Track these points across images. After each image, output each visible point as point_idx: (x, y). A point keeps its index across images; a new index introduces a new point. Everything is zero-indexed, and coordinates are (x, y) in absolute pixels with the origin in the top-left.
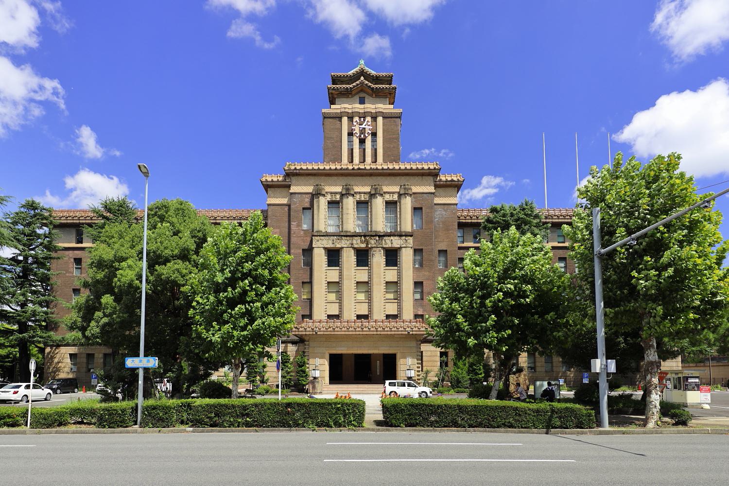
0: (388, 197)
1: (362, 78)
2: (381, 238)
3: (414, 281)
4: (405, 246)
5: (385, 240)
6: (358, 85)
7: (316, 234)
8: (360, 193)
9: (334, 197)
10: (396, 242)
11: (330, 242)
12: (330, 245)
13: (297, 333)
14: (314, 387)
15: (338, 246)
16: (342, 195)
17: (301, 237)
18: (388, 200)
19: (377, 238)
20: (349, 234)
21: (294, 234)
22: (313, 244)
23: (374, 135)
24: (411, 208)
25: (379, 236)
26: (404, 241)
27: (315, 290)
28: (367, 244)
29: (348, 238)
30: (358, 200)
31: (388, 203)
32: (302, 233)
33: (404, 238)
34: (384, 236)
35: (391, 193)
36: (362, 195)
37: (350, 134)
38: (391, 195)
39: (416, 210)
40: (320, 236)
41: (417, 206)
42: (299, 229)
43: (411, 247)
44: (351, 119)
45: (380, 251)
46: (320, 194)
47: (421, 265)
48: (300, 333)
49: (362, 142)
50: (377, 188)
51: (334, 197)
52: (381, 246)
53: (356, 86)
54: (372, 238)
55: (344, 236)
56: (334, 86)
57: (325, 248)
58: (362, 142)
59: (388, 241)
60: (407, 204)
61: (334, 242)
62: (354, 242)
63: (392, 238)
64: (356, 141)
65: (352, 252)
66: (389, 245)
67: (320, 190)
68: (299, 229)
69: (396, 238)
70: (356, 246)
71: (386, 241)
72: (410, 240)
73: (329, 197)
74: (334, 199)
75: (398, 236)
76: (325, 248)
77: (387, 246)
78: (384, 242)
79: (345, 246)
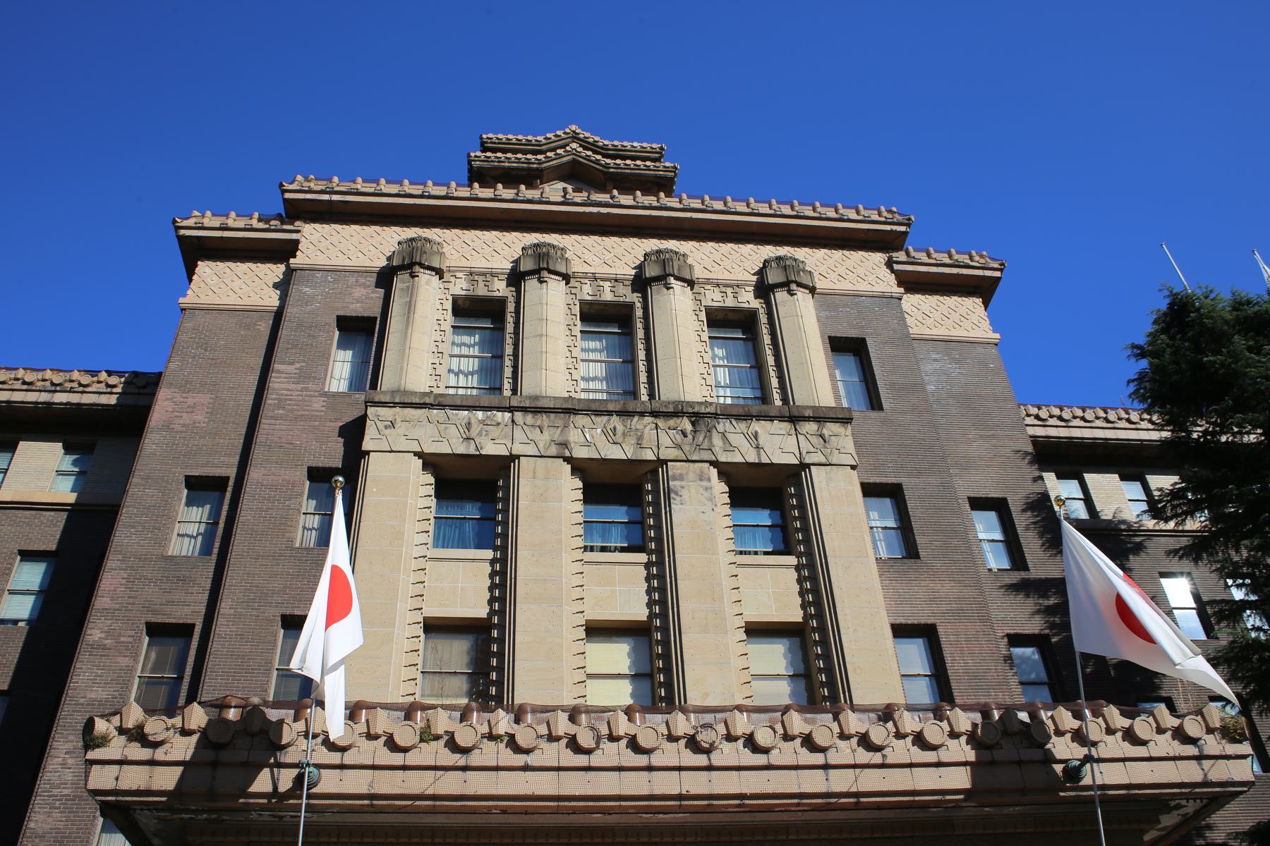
0: (714, 298)
2: (702, 427)
3: (893, 621)
4: (823, 460)
5: (723, 435)
7: (387, 399)
8: (595, 278)
9: (481, 284)
18: (715, 304)
19: (686, 425)
22: (367, 438)
25: (697, 417)
26: (815, 440)
28: (639, 444)
29: (544, 420)
31: (719, 320)
32: (318, 404)
33: (811, 427)
34: (715, 416)
35: (726, 286)
36: (607, 284)
38: (729, 290)
40: (405, 405)
42: (307, 389)
43: (853, 467)
45: (702, 477)
47: (911, 552)
52: (707, 456)
54: (661, 423)
55: (524, 410)
57: (430, 462)
61: (474, 433)
62: (574, 436)
63: (757, 426)
65: (570, 487)
68: (307, 389)
69: (782, 427)
70: (581, 453)
71: (730, 437)
72: (843, 440)
73: (460, 287)
74: (481, 291)
75: (781, 418)
76: (430, 462)
77: (738, 459)
78: (717, 441)
79: (531, 450)
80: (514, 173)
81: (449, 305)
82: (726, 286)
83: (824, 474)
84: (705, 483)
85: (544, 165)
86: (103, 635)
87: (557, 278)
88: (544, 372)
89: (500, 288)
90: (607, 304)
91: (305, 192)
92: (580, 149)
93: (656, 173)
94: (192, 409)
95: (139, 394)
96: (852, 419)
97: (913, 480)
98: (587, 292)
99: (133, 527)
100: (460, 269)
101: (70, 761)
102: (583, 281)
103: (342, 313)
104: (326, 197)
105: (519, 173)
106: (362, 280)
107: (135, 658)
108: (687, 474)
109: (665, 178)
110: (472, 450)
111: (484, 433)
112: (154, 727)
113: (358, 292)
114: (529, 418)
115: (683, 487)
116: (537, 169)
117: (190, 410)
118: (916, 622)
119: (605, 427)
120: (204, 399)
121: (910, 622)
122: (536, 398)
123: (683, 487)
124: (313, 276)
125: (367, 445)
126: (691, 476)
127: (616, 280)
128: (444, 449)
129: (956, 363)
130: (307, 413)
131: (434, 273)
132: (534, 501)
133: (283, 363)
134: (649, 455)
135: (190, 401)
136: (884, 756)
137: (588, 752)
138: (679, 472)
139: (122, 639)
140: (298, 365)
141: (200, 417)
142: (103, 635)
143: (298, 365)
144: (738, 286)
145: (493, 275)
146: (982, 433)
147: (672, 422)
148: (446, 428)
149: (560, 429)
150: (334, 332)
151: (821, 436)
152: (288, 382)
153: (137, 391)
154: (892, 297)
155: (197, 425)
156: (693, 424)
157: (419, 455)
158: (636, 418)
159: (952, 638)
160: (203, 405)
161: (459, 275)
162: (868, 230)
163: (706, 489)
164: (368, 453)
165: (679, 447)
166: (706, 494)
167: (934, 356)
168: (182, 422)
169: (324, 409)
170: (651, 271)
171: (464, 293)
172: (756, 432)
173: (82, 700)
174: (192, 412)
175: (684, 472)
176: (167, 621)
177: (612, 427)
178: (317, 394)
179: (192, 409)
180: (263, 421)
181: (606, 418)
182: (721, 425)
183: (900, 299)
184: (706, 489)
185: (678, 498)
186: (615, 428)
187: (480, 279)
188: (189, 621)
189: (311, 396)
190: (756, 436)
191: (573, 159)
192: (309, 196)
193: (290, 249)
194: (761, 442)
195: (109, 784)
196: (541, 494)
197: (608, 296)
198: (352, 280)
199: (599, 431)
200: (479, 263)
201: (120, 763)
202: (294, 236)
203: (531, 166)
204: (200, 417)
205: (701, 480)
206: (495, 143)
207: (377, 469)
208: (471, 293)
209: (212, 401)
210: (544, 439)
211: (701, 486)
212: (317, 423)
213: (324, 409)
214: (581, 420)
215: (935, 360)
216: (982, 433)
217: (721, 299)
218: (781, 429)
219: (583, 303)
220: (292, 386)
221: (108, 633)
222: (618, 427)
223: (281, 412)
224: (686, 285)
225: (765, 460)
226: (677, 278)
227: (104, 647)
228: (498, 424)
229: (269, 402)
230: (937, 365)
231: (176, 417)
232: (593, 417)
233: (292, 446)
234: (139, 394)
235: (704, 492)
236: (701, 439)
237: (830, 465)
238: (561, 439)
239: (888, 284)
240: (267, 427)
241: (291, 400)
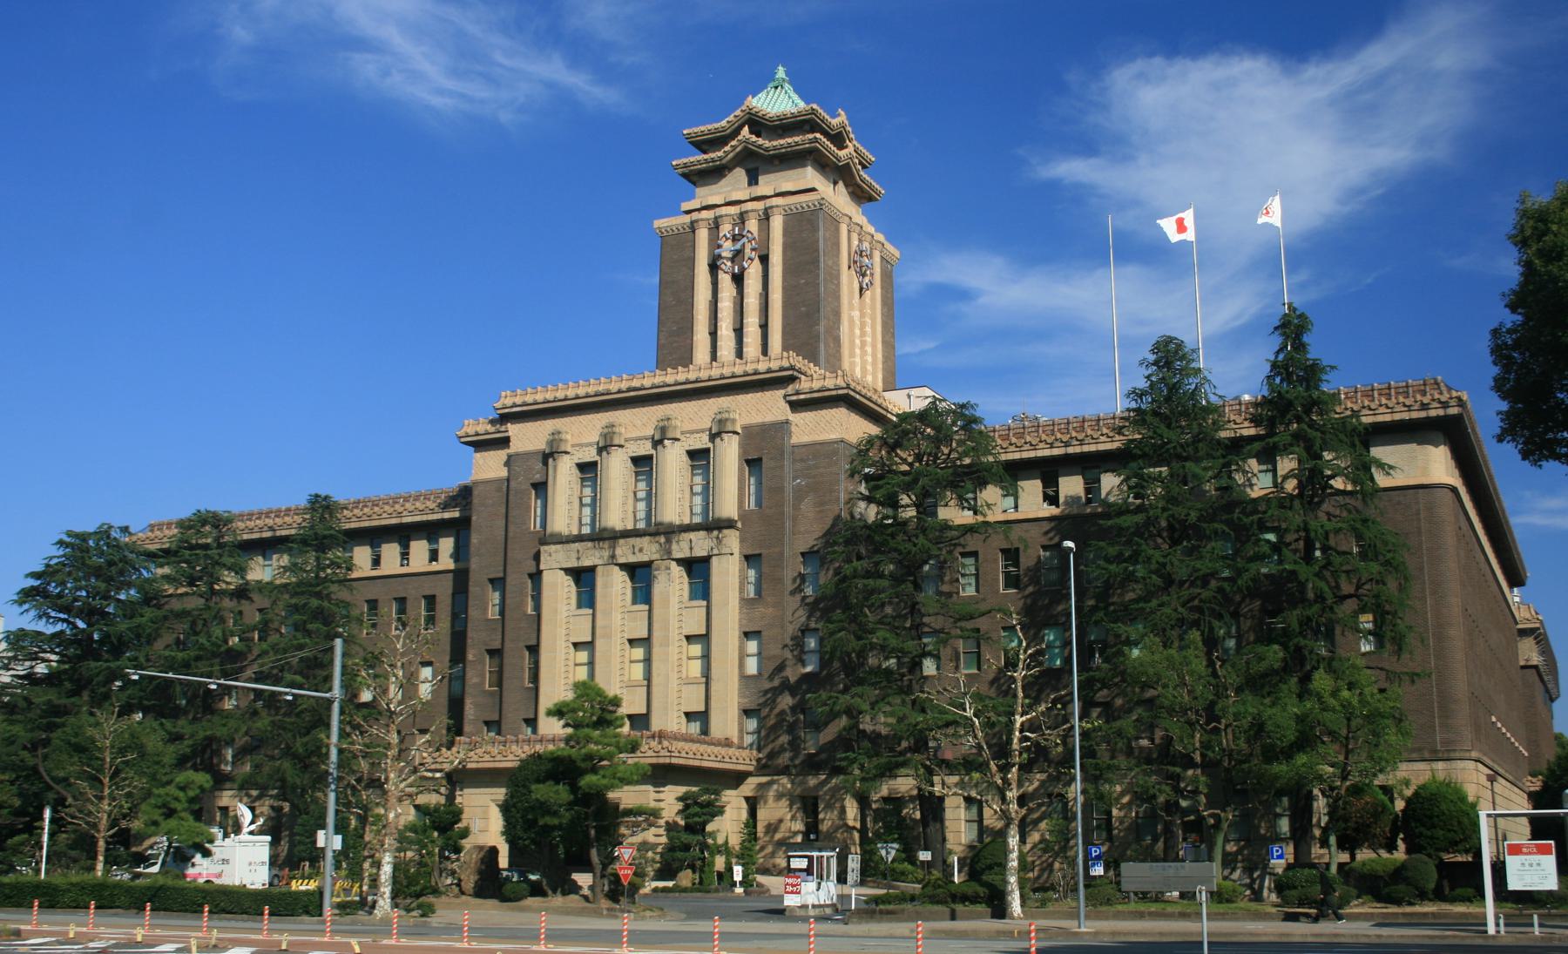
6: (734, 147)
10: (700, 544)
11: (574, 555)
12: (573, 564)
15: (587, 563)
19: (662, 539)
23: (764, 259)
37: (714, 268)
39: (752, 463)
49: (738, 279)
57: (568, 571)
58: (738, 279)
60: (673, 461)
64: (725, 280)
69: (702, 533)
76: (568, 571)
107: (484, 665)
126: (663, 568)
147: (657, 538)
150: (530, 493)
157: (561, 569)
193: (504, 442)
202: (506, 434)
210: (606, 554)
221: (474, 655)
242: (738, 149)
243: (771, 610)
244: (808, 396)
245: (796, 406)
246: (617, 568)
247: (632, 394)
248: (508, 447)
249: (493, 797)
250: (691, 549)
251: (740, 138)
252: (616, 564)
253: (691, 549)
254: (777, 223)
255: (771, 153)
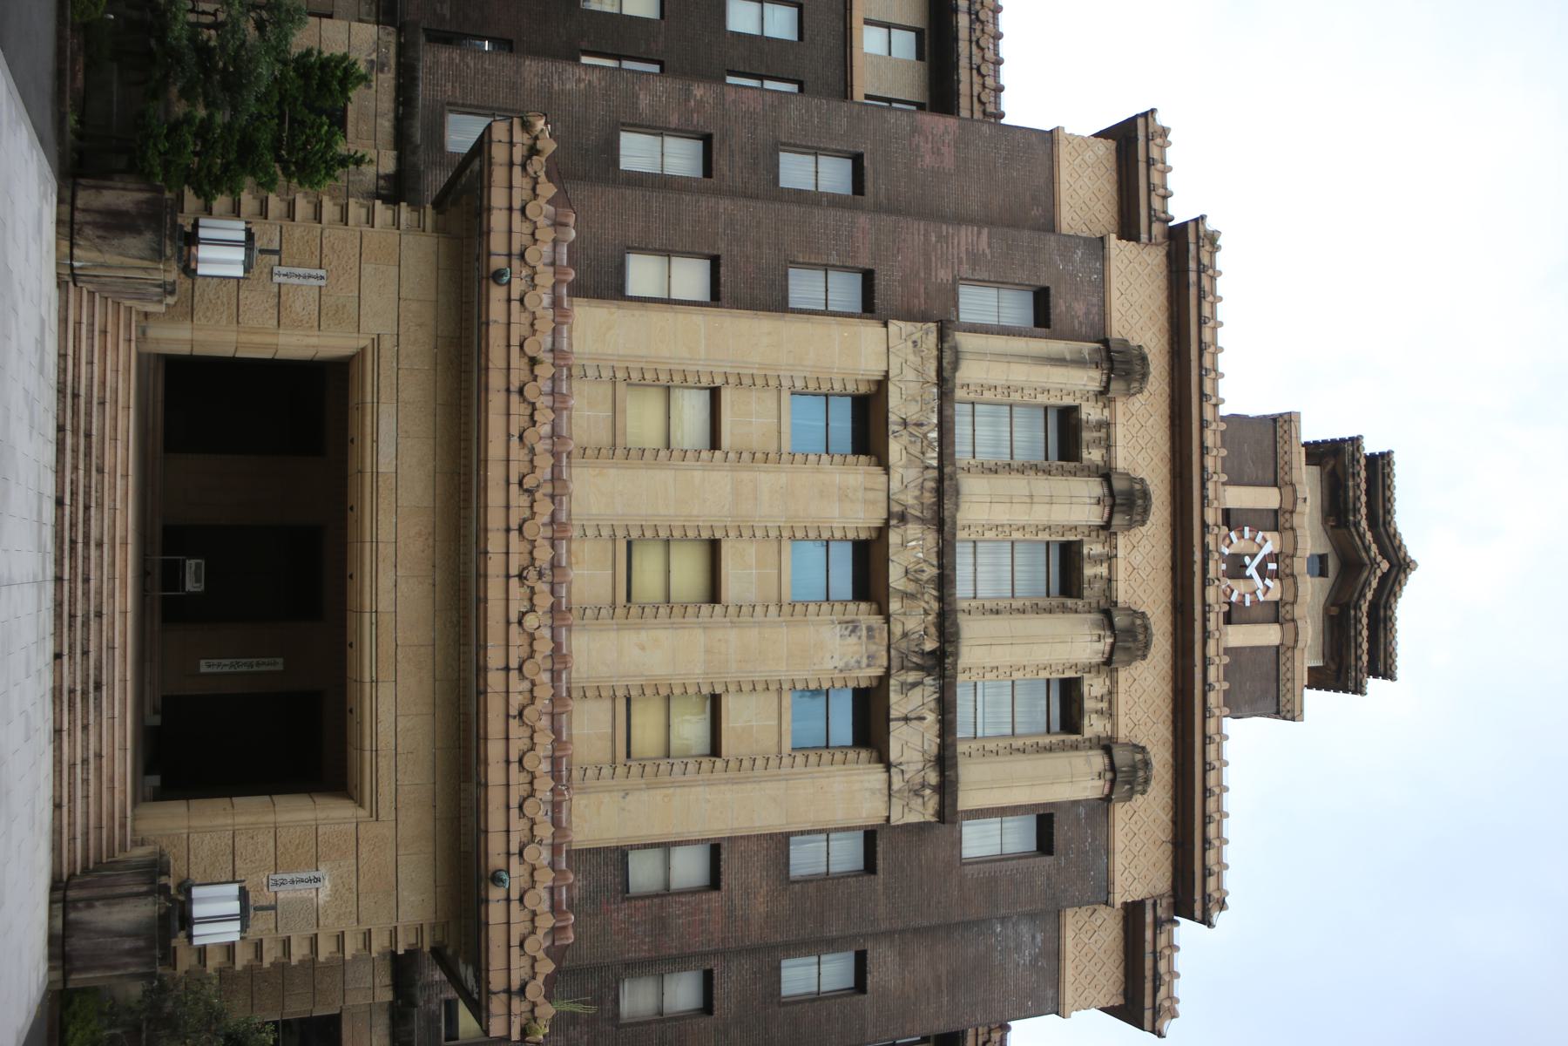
0: (1094, 687)
1: (1385, 566)
2: (930, 662)
3: (725, 845)
4: (895, 787)
6: (1367, 550)
8: (1110, 558)
9: (1096, 434)
11: (913, 412)
12: (898, 405)
13: (499, 153)
14: (115, 224)
15: (895, 449)
16: (1106, 474)
17: (928, 268)
18: (1086, 689)
19: (930, 645)
20: (948, 505)
21: (940, 237)
22: (901, 324)
24: (1052, 804)
27: (680, 316)
28: (905, 595)
29: (929, 498)
30: (1085, 551)
32: (944, 275)
33: (933, 778)
35: (1110, 702)
38: (1104, 705)
41: (1060, 833)
42: (960, 263)
44: (1275, 520)
46: (1111, 370)
48: (499, 174)
50: (1135, 639)
51: (1096, 434)
52: (895, 663)
53: (1363, 543)
56: (1363, 461)
59: (916, 696)
61: (911, 429)
62: (913, 530)
63: (931, 718)
66: (899, 704)
67: (1128, 374)
68: (960, 263)
69: (932, 744)
70: (894, 538)
71: (918, 691)
72: (921, 811)
73: (1091, 412)
74: (1086, 435)
77: (894, 697)
78: (912, 677)
79: (895, 485)
80: (1341, 492)
81: (1068, 401)
82: (1110, 702)
83: (878, 787)
84: (864, 661)
85: (1353, 530)
86: (698, 97)
87: (1106, 515)
88: (989, 500)
89: (1093, 455)
90: (1080, 570)
91: (1197, 243)
92: (1379, 573)
93: (1353, 668)
94: (937, 152)
95: (972, 96)
96: (944, 823)
97: (880, 888)
98: (1093, 548)
99: (807, 111)
100: (1113, 414)
101: (582, 86)
102: (1107, 545)
103: (1052, 292)
104: (1192, 265)
105: (1341, 499)
106: (1095, 310)
108: (875, 643)
109: (1347, 679)
110: (892, 428)
111: (913, 439)
112: (538, 164)
113: (1080, 308)
114: (931, 485)
115: (860, 638)
116: (1348, 521)
117: (935, 150)
118: (722, 869)
119: (925, 561)
120: (949, 162)
121: (722, 863)
122: (957, 492)
123: (860, 638)
124: (1096, 260)
125: (895, 326)
126: (873, 648)
127: (1110, 580)
128: (894, 401)
129: (1030, 961)
130: (934, 265)
131: (1103, 384)
132: (840, 489)
133: (990, 237)
134: (895, 606)
135: (945, 150)
136: (515, 717)
137: (521, 484)
138: (877, 635)
139: (695, 115)
140: (987, 251)
141: (928, 160)
142: (698, 97)
143: (987, 251)
144: (1110, 714)
145: (1108, 447)
146: (944, 978)
147: (932, 630)
148: (917, 401)
149: (919, 515)
151: (923, 786)
152: (967, 244)
153: (975, 94)
154: (1109, 893)
155: (919, 159)
156: (932, 653)
158: (935, 593)
159: (705, 906)
160: (942, 162)
161: (1106, 412)
162: (1193, 873)
163: (858, 662)
164: (886, 325)
165: (905, 635)
166: (852, 662)
167: (1039, 938)
168: (922, 144)
169: (939, 280)
170: (1119, 620)
171: (1084, 417)
172: (924, 718)
173: (637, 88)
174: (933, 153)
175: (877, 640)
176: (714, 153)
177: (925, 569)
178: (956, 272)
179: (937, 152)
180: (922, 224)
181: (935, 563)
182: (932, 682)
183: (1107, 903)
184: (858, 662)
185: (847, 633)
186: (923, 571)
187: (1103, 434)
188: (714, 173)
189: (953, 268)
190: (922, 719)
191: (1366, 565)
192: (1192, 247)
194: (915, 723)
195: (495, 137)
196: (847, 496)
197: (1089, 571)
198: (1095, 300)
199: (921, 555)
200: (1120, 434)
201: (511, 144)
203: (1351, 513)
204: (928, 160)
205: (868, 657)
206: (1383, 469)
207: (870, 332)
208: (1084, 424)
209: (947, 171)
210: (909, 498)
211: (861, 657)
212: (922, 275)
213: (939, 280)
214: (931, 538)
215: (1034, 937)
216: (944, 978)
217: (1093, 694)
218: (930, 746)
219: (1080, 543)
220: (963, 249)
221: (700, 103)
222: (925, 574)
223: (934, 239)
224: (1106, 656)
225: (893, 725)
226: (1113, 646)
227: (687, 100)
228: (923, 453)
229: (944, 227)
230: (1027, 938)
231: (927, 138)
232: (936, 549)
233: (895, 252)
234: (972, 96)
235: (854, 659)
236: (915, 659)
237: (890, 795)
238: (909, 516)
239: (1127, 887)
240: (916, 226)
241: (947, 247)
242: (1364, 554)
243: (762, 909)
244: (1148, 948)
245: (1133, 914)
246: (878, 523)
247: (1197, 556)
248: (1120, 237)
249: (387, 344)
250: (906, 719)
251: (1379, 558)
252: (887, 521)
253: (906, 719)
254: (1269, 635)
255: (1352, 612)
